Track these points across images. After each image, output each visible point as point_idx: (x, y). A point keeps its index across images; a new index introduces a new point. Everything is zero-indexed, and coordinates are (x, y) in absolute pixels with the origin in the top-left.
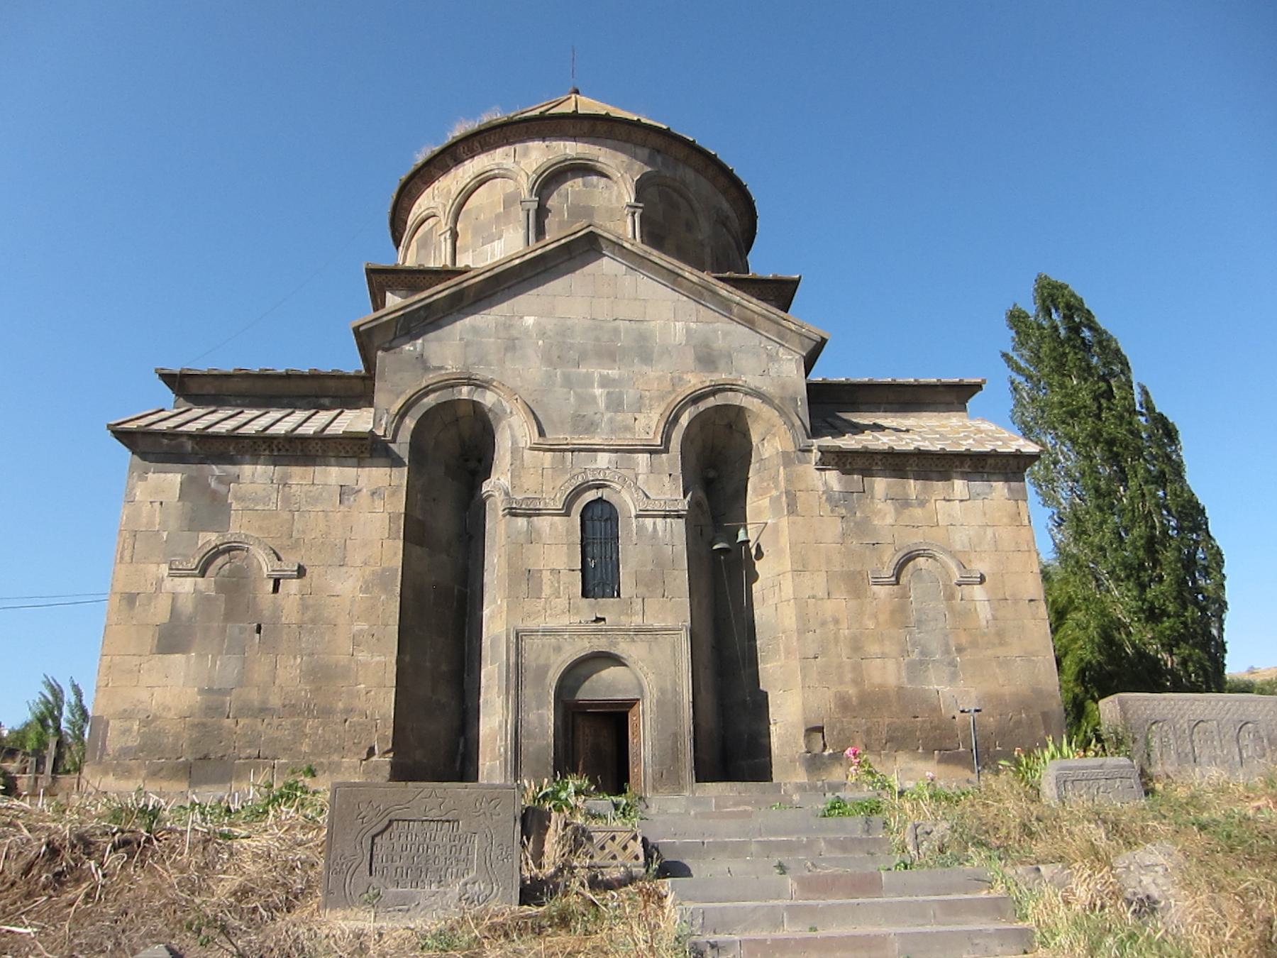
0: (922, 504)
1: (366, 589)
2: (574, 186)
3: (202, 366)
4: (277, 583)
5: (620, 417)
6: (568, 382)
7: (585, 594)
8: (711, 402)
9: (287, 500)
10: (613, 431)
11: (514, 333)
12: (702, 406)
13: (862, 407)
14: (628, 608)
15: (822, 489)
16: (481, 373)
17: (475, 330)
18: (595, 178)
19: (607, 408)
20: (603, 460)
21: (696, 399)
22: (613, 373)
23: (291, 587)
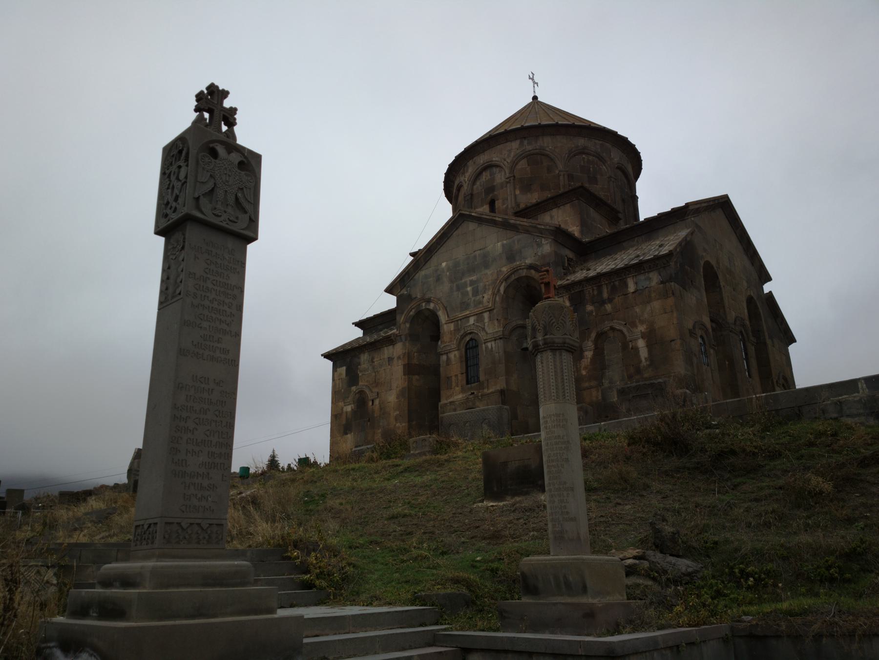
0: (610, 300)
1: (397, 398)
2: (485, 176)
3: (364, 317)
4: (373, 401)
5: (478, 298)
6: (458, 288)
7: (468, 383)
8: (513, 277)
9: (373, 368)
12: (509, 281)
16: (427, 297)
17: (426, 277)
18: (494, 169)
19: (473, 295)
20: (472, 320)
21: (506, 279)
22: (474, 278)
23: (377, 402)
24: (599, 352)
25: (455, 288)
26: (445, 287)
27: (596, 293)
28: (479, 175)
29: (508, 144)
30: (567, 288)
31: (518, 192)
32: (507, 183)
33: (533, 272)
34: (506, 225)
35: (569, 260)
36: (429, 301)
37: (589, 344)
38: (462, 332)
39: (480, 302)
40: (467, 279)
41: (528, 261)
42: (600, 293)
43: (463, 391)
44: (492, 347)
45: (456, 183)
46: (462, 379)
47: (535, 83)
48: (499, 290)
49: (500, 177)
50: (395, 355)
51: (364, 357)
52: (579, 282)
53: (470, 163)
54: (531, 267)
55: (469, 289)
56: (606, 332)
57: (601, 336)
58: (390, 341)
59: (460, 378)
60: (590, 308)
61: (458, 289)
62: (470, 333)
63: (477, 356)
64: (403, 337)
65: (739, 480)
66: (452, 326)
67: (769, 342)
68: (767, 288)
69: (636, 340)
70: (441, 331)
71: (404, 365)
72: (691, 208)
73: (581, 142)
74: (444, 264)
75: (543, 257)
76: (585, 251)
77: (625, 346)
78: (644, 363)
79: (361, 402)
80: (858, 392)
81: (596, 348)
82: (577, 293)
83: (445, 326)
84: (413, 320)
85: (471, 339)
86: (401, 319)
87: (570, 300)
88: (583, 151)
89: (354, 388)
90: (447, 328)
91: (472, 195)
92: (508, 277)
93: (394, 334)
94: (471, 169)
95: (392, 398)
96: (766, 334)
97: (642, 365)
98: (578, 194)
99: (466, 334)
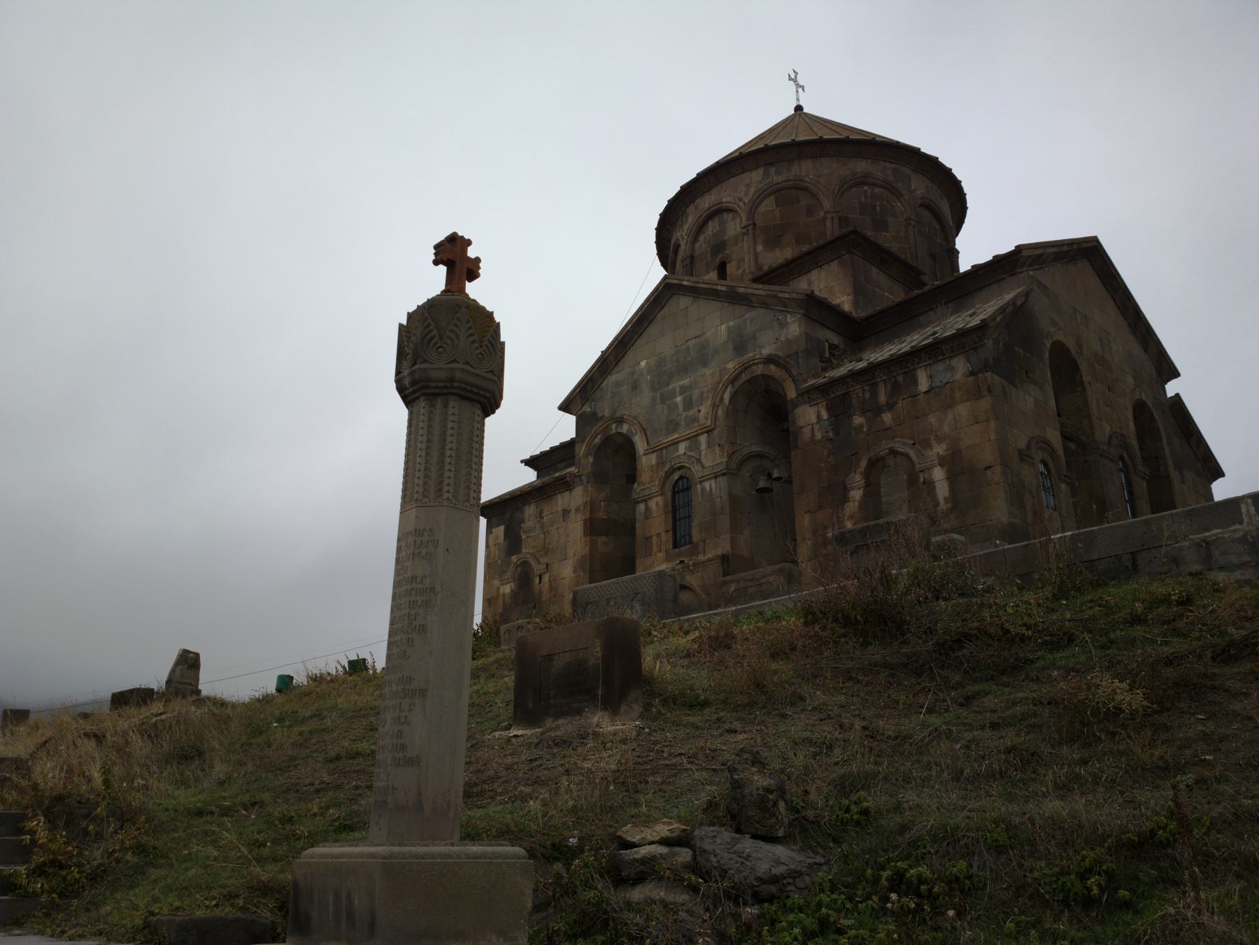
0: (890, 406)
1: (575, 572)
2: (712, 227)
5: (691, 412)
6: (663, 399)
7: (675, 546)
8: (744, 378)
9: (542, 527)
10: (687, 425)
11: (636, 376)
12: (737, 384)
13: (921, 319)
14: (695, 551)
15: (815, 420)
17: (618, 384)
18: (725, 216)
20: (682, 448)
22: (686, 382)
23: (546, 578)
24: (872, 490)
25: (658, 400)
26: (645, 397)
27: (867, 395)
28: (701, 227)
29: (747, 174)
30: (823, 389)
31: (760, 248)
32: (744, 234)
33: (772, 367)
34: (733, 298)
35: (832, 347)
36: (620, 421)
37: (857, 479)
38: (667, 467)
39: (695, 419)
40: (677, 385)
41: (766, 351)
42: (875, 395)
43: (668, 558)
44: (711, 490)
45: (673, 241)
46: (667, 539)
47: (798, 86)
48: (722, 399)
49: (733, 227)
50: (573, 507)
51: (530, 511)
52: (842, 380)
53: (691, 208)
54: (770, 360)
55: (679, 399)
56: (883, 459)
57: (872, 464)
58: (565, 485)
59: (664, 538)
60: (858, 420)
61: (663, 399)
62: (680, 468)
63: (689, 504)
64: (584, 478)
65: (977, 687)
66: (653, 459)
67: (1175, 475)
68: (1172, 388)
69: (930, 469)
70: (639, 467)
71: (585, 522)
72: (1025, 253)
73: (861, 166)
74: (643, 363)
75: (789, 342)
76: (859, 332)
77: (913, 479)
78: (943, 506)
79: (525, 579)
80: (1241, 523)
81: (868, 485)
82: (837, 398)
83: (644, 459)
84: (599, 451)
85: (681, 478)
86: (581, 450)
87: (828, 409)
88: (863, 181)
89: (514, 558)
90: (646, 461)
91: (692, 257)
92: (736, 377)
93: (570, 473)
94: (692, 217)
95: (567, 572)
96: (1170, 462)
97: (939, 509)
98: (850, 245)
99: (673, 470)
